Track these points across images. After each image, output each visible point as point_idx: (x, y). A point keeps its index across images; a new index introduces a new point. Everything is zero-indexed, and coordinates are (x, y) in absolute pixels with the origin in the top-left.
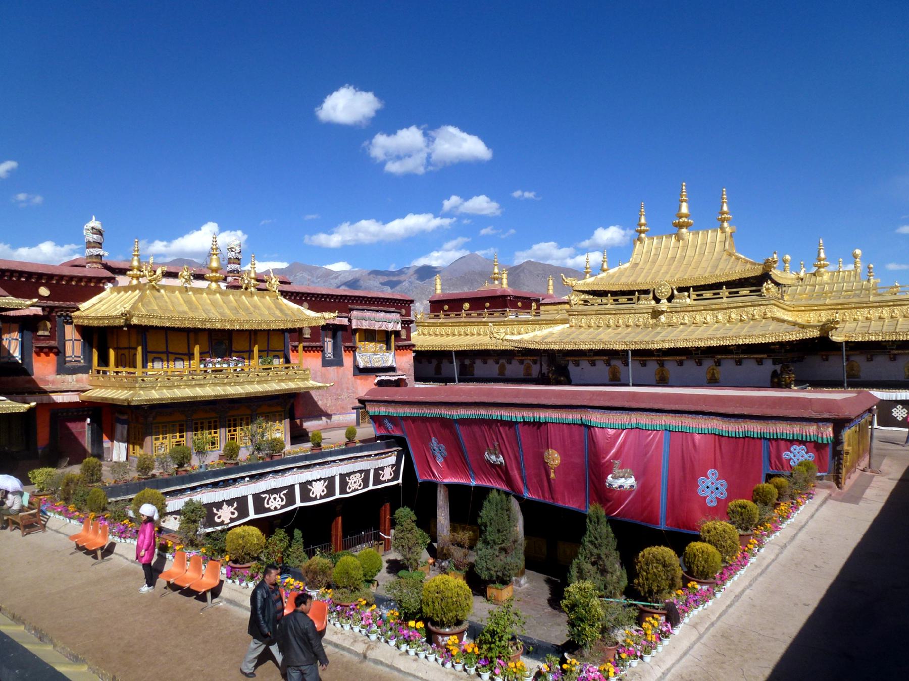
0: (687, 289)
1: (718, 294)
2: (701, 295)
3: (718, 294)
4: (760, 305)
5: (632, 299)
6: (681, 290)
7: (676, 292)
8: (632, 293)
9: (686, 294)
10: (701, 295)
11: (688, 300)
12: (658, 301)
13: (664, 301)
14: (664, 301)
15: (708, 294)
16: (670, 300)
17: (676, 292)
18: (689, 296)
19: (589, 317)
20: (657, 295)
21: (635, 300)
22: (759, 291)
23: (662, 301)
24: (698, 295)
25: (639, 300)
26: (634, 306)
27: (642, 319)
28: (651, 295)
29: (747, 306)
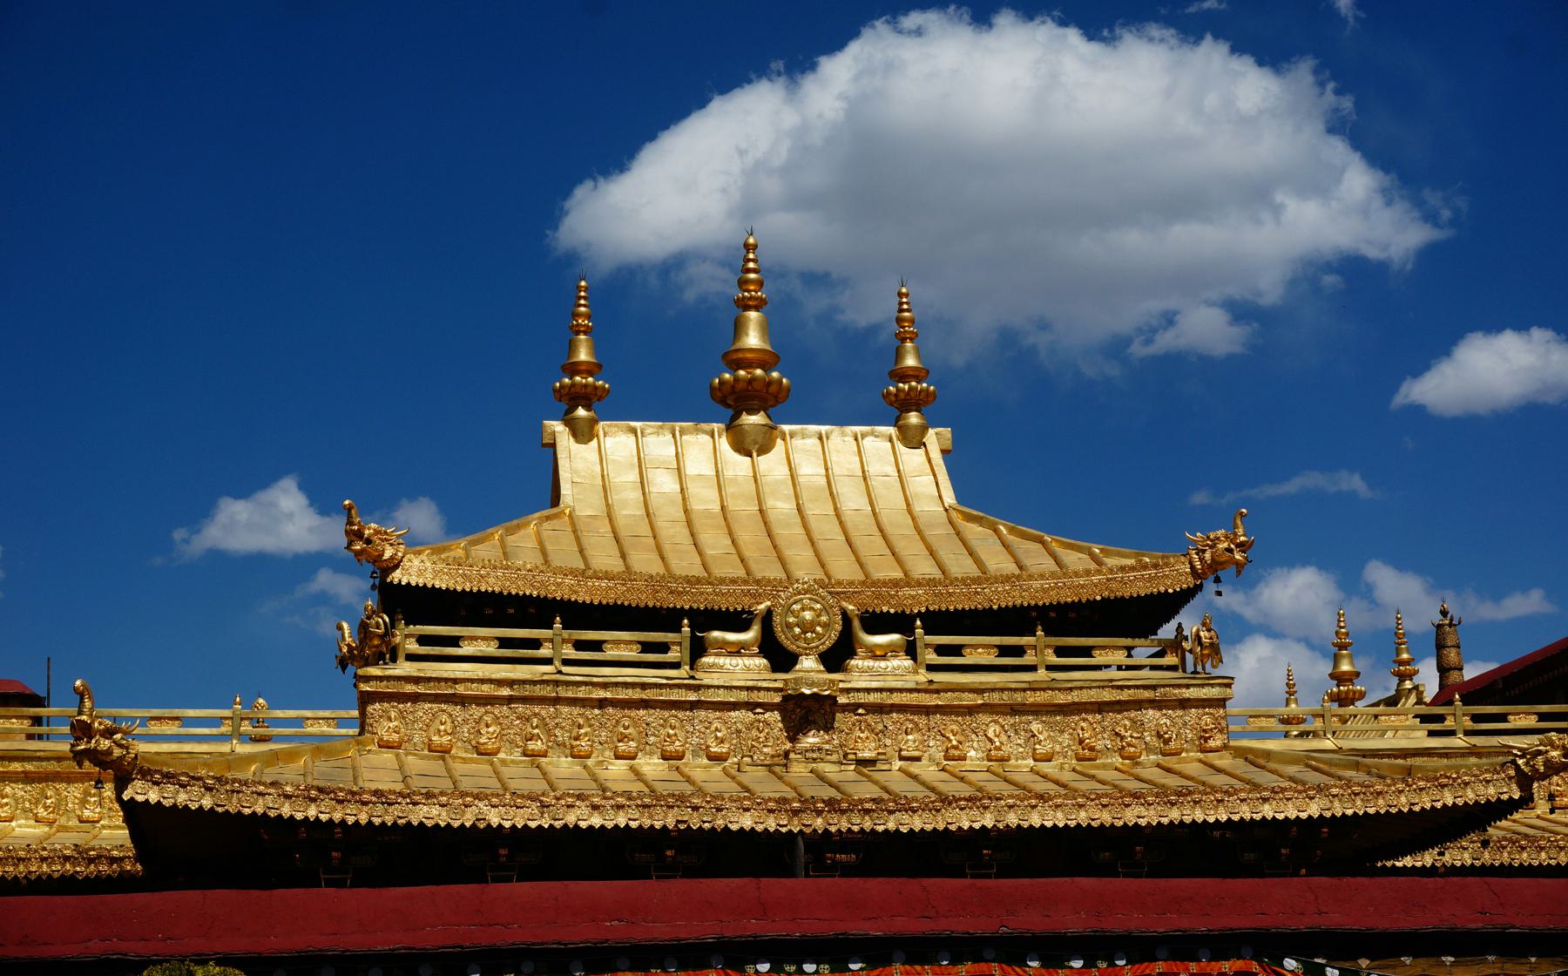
0: (899, 622)
1: (1019, 651)
2: (956, 650)
3: (1019, 651)
4: (1184, 704)
5: (663, 648)
8: (665, 619)
10: (956, 650)
11: (908, 663)
12: (781, 659)
13: (808, 663)
14: (808, 663)
15: (980, 649)
16: (836, 658)
18: (911, 651)
19: (476, 711)
24: (941, 650)
27: (717, 729)
29: (1138, 705)
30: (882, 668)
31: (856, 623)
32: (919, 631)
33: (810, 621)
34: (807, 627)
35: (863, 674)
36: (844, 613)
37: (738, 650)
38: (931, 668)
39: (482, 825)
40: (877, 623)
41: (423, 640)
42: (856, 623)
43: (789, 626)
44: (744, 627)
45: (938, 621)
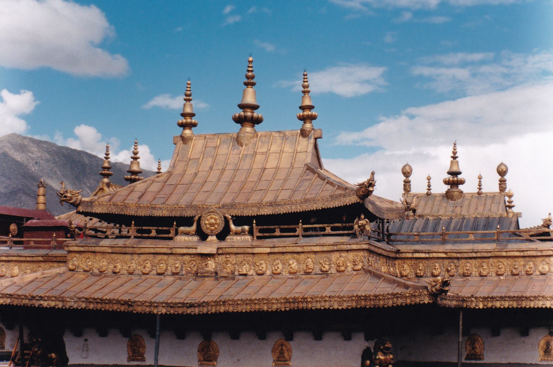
6: (239, 220)
7: (233, 227)
9: (246, 228)
11: (249, 238)
12: (203, 236)
16: (222, 236)
17: (233, 227)
18: (251, 232)
20: (204, 228)
21: (173, 232)
22: (351, 228)
23: (210, 238)
25: (177, 233)
26: (170, 244)
28: (194, 227)
30: (239, 240)
31: (231, 222)
32: (254, 225)
33: (212, 222)
34: (212, 225)
35: (233, 240)
36: (225, 218)
37: (187, 234)
38: (258, 238)
39: (64, 308)
40: (239, 220)
41: (35, 242)
42: (231, 222)
43: (206, 224)
44: (191, 225)
45: (262, 220)
